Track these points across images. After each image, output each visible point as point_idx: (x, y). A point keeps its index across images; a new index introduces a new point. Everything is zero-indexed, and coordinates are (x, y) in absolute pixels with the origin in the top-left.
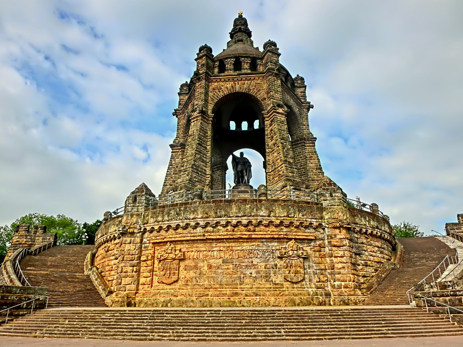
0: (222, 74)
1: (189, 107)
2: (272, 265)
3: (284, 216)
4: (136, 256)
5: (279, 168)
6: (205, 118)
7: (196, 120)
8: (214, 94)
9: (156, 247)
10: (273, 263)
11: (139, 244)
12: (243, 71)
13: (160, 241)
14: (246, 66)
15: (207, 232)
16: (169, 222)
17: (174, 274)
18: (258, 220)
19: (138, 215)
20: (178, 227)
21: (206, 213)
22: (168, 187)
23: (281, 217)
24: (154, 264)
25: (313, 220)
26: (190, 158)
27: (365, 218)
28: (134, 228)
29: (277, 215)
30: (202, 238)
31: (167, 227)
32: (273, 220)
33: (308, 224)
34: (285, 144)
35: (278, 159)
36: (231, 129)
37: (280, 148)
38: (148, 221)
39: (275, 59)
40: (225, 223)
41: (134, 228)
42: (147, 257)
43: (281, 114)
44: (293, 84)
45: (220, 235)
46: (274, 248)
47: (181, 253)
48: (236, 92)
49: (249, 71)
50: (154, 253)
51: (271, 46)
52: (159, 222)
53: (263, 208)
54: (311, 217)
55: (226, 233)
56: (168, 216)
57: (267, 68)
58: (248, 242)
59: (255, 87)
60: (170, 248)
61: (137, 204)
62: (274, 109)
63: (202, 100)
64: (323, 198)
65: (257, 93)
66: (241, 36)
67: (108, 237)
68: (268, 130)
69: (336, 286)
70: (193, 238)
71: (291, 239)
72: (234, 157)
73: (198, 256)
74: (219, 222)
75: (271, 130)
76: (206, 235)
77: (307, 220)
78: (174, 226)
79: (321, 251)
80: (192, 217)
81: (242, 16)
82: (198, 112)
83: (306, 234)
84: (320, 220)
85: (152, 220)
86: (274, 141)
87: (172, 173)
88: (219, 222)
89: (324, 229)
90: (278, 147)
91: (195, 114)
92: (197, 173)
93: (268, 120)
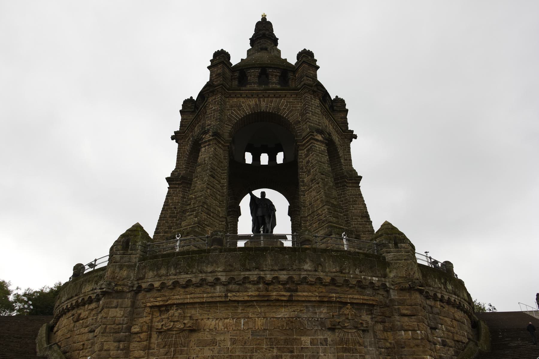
0: (244, 88)
1: (196, 129)
2: (321, 339)
3: (337, 272)
4: (124, 326)
5: (319, 211)
6: (220, 143)
7: (208, 145)
8: (232, 113)
9: (155, 313)
10: (321, 337)
11: (129, 309)
12: (271, 86)
13: (161, 303)
14: (274, 80)
15: (231, 291)
16: (176, 277)
17: (181, 352)
18: (302, 276)
19: (129, 267)
20: (189, 283)
21: (230, 265)
22: (161, 234)
23: (331, 272)
24: (150, 337)
25: (374, 278)
26: (199, 194)
27: (440, 279)
28: (124, 285)
29: (327, 270)
30: (223, 300)
31: (173, 283)
32: (321, 277)
33: (367, 284)
34: (326, 180)
35: (318, 199)
36: (247, 162)
37: (320, 184)
38: (144, 276)
39: (312, 72)
40: (256, 279)
41: (124, 285)
42: (141, 327)
43: (320, 141)
44: (332, 107)
45: (248, 296)
46: (322, 316)
47: (192, 321)
48: (261, 112)
49: (278, 87)
50: (152, 321)
51: (307, 58)
52: (160, 277)
53: (308, 260)
55: (257, 293)
56: (175, 268)
57: (302, 83)
58: (287, 306)
59: (286, 106)
60: (176, 314)
61: (130, 252)
62: (311, 135)
63: (216, 120)
64: (385, 250)
65: (288, 114)
66: (265, 44)
67: (81, 299)
68: (302, 162)
70: (211, 300)
71: (346, 303)
72: (253, 197)
73: (217, 327)
74: (248, 278)
75: (308, 162)
76: (229, 294)
77: (367, 277)
78: (183, 282)
79: (385, 322)
80: (209, 270)
81: (266, 19)
82: (210, 134)
83: (366, 297)
84: (383, 279)
85: (151, 274)
86: (310, 177)
87: (168, 216)
88: (248, 278)
89: (388, 291)
90: (318, 183)
91: (208, 137)
92: (207, 214)
93: (303, 150)
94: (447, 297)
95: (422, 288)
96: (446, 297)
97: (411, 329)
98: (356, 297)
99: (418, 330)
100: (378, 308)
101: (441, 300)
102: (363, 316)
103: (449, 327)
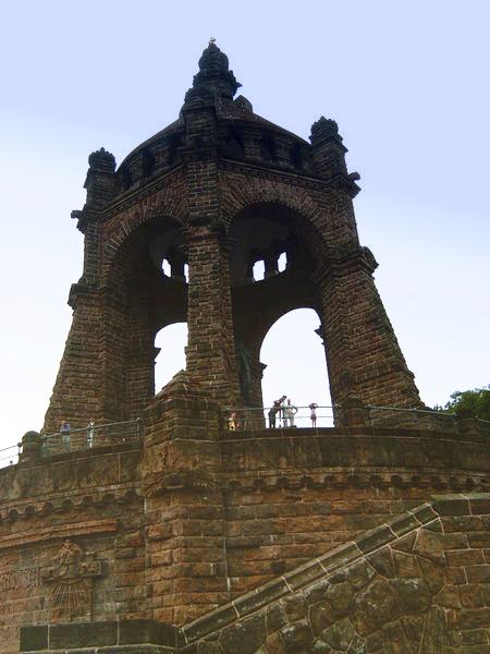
25: (112, 487)
43: (206, 237)
54: (106, 482)
71: (65, 539)
98: (80, 525)
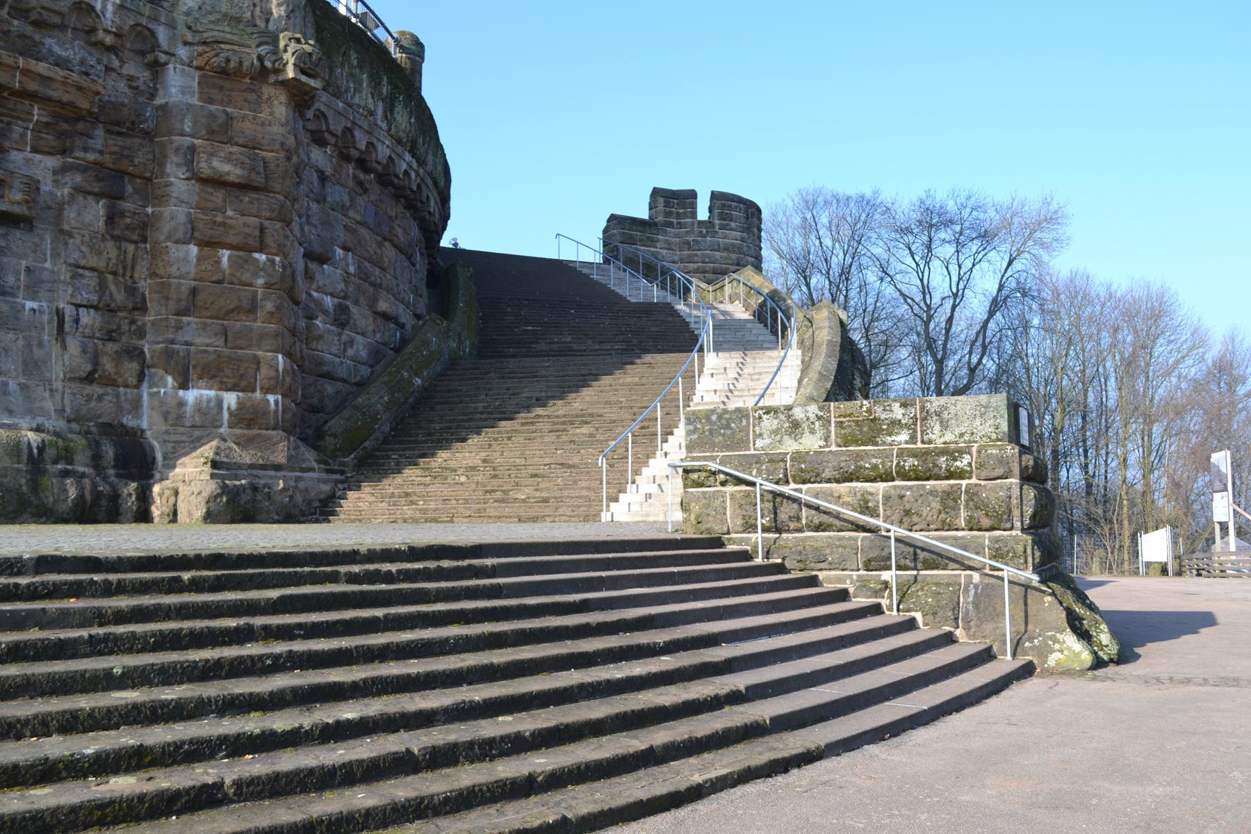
27: (375, 81)
69: (188, 410)
89: (156, 68)
94: (388, 152)
95: (312, 83)
96: (383, 152)
97: (231, 239)
99: (261, 251)
100: (100, 132)
101: (362, 164)
102: (14, 155)
103: (367, 264)
